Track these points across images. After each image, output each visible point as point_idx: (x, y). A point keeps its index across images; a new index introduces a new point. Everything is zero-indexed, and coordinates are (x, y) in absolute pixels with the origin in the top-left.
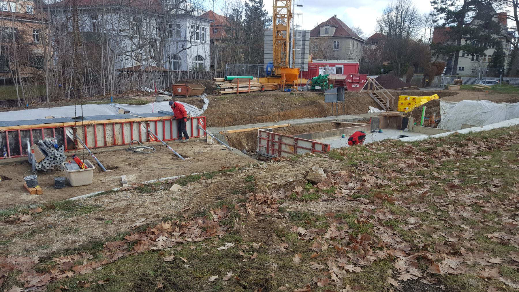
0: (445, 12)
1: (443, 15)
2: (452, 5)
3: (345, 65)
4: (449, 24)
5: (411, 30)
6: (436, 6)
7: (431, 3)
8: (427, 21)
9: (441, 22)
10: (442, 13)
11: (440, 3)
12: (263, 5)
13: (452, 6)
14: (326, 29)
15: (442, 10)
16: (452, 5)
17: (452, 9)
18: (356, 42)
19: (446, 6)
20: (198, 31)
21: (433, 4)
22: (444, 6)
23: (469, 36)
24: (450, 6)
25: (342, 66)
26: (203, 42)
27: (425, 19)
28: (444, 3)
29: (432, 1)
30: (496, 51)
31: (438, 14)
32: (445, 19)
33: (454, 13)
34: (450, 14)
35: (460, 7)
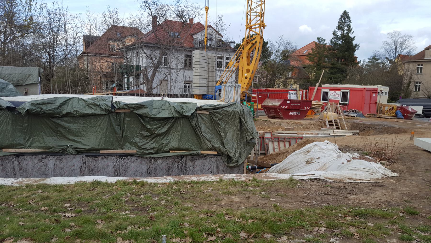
3: (351, 90)
12: (352, 31)
25: (348, 91)
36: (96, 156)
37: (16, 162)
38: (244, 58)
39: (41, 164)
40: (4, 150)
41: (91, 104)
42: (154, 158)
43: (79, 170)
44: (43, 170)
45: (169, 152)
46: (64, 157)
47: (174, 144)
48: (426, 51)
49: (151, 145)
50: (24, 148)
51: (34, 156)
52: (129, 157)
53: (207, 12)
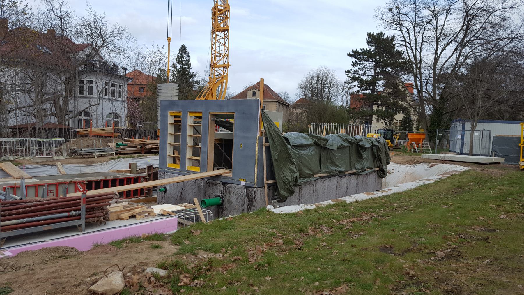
0: (358, 81)
1: (356, 83)
2: (364, 74)
4: (362, 91)
5: (331, 96)
6: (350, 75)
7: (345, 71)
8: (343, 88)
9: (356, 89)
10: (355, 81)
11: (353, 72)
13: (364, 75)
14: (253, 92)
15: (354, 79)
16: (364, 74)
17: (364, 78)
18: (281, 106)
19: (359, 75)
20: (107, 87)
21: (347, 73)
22: (357, 76)
23: (380, 102)
24: (362, 75)
26: (114, 98)
27: (342, 87)
28: (357, 73)
29: (346, 71)
30: (404, 116)
31: (352, 82)
32: (359, 87)
33: (366, 81)
34: (362, 83)
35: (371, 76)
36: (341, 177)
37: (314, 185)
38: (213, 95)
39: (323, 185)
40: (315, 176)
41: (344, 139)
42: (359, 175)
43: (335, 188)
44: (324, 189)
45: (365, 170)
46: (331, 178)
47: (367, 165)
48: (248, 92)
49: (359, 166)
50: (321, 174)
51: (321, 179)
52: (352, 176)
53: (169, 43)
